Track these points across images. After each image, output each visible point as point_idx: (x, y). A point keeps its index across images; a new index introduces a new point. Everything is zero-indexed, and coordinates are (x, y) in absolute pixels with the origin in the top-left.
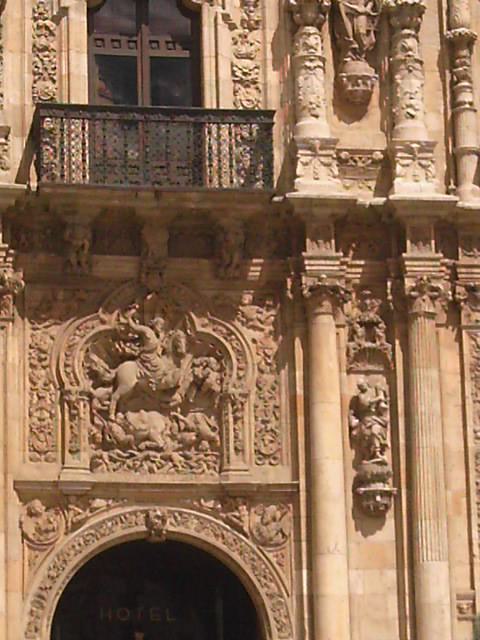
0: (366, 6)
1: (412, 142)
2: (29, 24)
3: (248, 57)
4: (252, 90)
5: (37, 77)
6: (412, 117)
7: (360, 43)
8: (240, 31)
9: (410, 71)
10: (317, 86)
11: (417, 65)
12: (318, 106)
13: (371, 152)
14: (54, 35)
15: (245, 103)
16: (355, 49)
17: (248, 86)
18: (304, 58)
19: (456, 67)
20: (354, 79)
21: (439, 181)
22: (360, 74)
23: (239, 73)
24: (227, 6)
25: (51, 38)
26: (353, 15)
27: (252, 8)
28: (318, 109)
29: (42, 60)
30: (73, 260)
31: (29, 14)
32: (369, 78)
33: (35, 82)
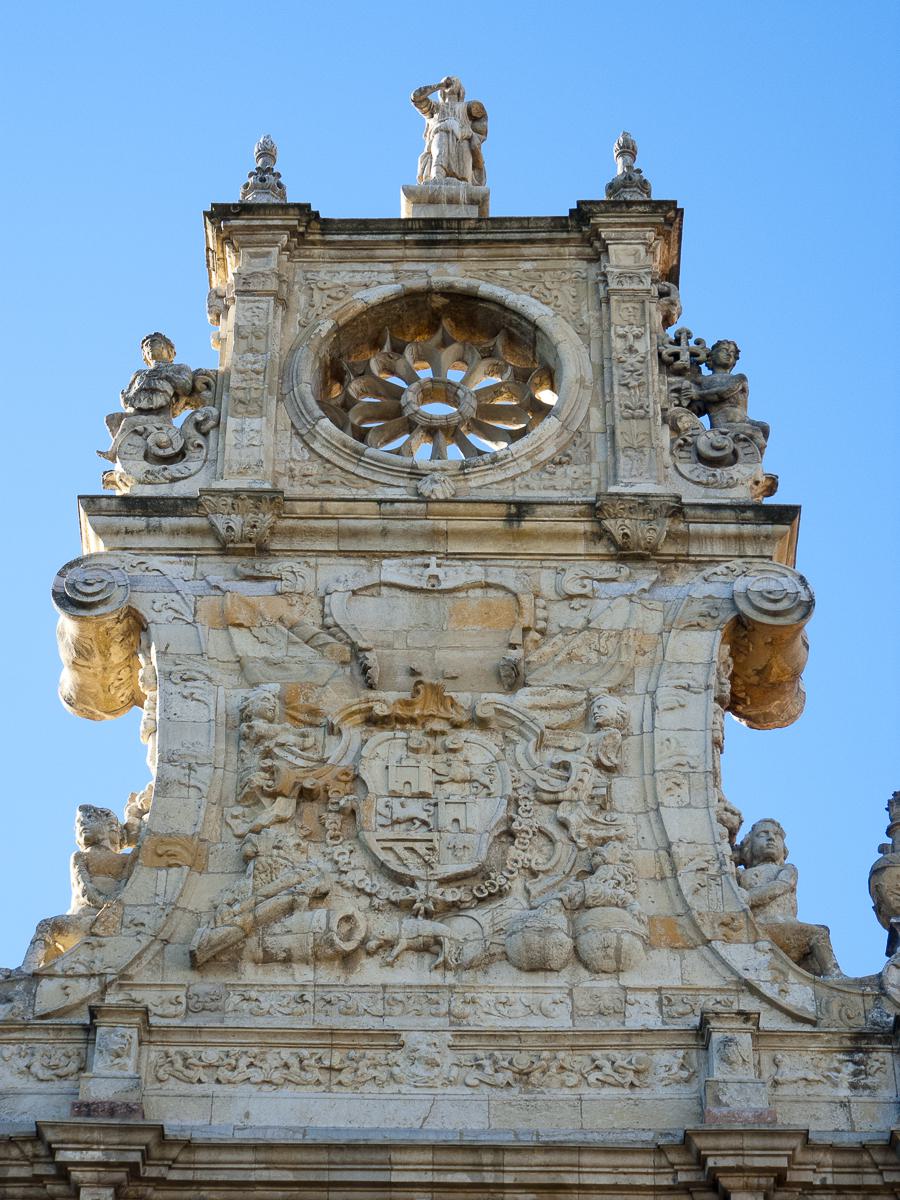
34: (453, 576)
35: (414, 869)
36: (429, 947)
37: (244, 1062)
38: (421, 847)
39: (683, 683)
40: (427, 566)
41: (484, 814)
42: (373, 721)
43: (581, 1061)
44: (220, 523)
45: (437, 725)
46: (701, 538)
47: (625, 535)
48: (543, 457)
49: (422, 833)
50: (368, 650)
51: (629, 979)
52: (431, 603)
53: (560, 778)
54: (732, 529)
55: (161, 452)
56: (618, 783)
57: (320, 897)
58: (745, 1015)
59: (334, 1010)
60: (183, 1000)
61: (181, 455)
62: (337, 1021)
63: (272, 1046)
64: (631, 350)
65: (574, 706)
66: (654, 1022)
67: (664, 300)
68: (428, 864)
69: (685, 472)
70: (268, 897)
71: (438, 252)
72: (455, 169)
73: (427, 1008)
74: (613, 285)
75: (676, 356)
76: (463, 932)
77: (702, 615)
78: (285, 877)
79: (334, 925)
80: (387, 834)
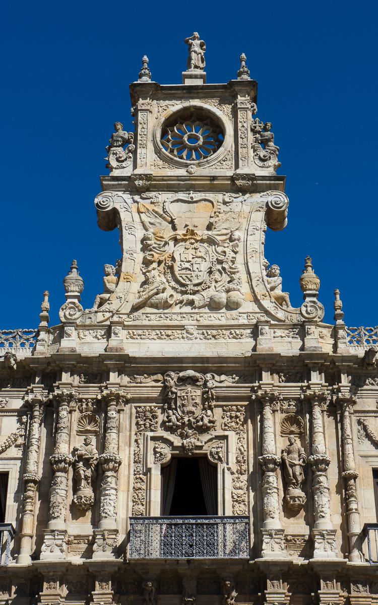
0: (299, 460)
1: (324, 530)
2: (132, 477)
3: (240, 488)
4: (242, 505)
5: (135, 503)
6: (323, 517)
7: (297, 481)
8: (237, 475)
9: (321, 493)
10: (274, 502)
11: (326, 490)
12: (273, 512)
13: (304, 536)
14: (144, 482)
15: (239, 512)
16: (294, 482)
17: (239, 503)
18: (267, 488)
19: (348, 491)
20: (293, 498)
21: (338, 550)
22: (296, 496)
23: (235, 497)
24: (230, 463)
25: (142, 483)
26: (293, 465)
27: (242, 464)
28: (274, 514)
29: (137, 495)
30: (147, 599)
31: (132, 472)
32: (301, 497)
33: (133, 506)
34: (197, 196)
35: (189, 283)
36: (191, 303)
37: (147, 333)
38: (189, 276)
39: (255, 227)
40: (189, 194)
41: (204, 266)
42: (176, 240)
43: (227, 332)
45: (193, 241)
47: (241, 185)
49: (189, 272)
50: (175, 219)
51: (240, 310)
53: (223, 255)
55: (120, 159)
56: (238, 256)
58: (267, 322)
59: (168, 319)
60: (132, 317)
62: (168, 322)
63: (154, 330)
64: (243, 126)
65: (228, 234)
66: (246, 322)
67: (252, 109)
68: (191, 281)
69: (257, 163)
70: (152, 290)
72: (197, 64)
73: (191, 319)
74: (239, 106)
75: (255, 127)
77: (260, 207)
78: (156, 285)
79: (168, 297)
80: (180, 272)
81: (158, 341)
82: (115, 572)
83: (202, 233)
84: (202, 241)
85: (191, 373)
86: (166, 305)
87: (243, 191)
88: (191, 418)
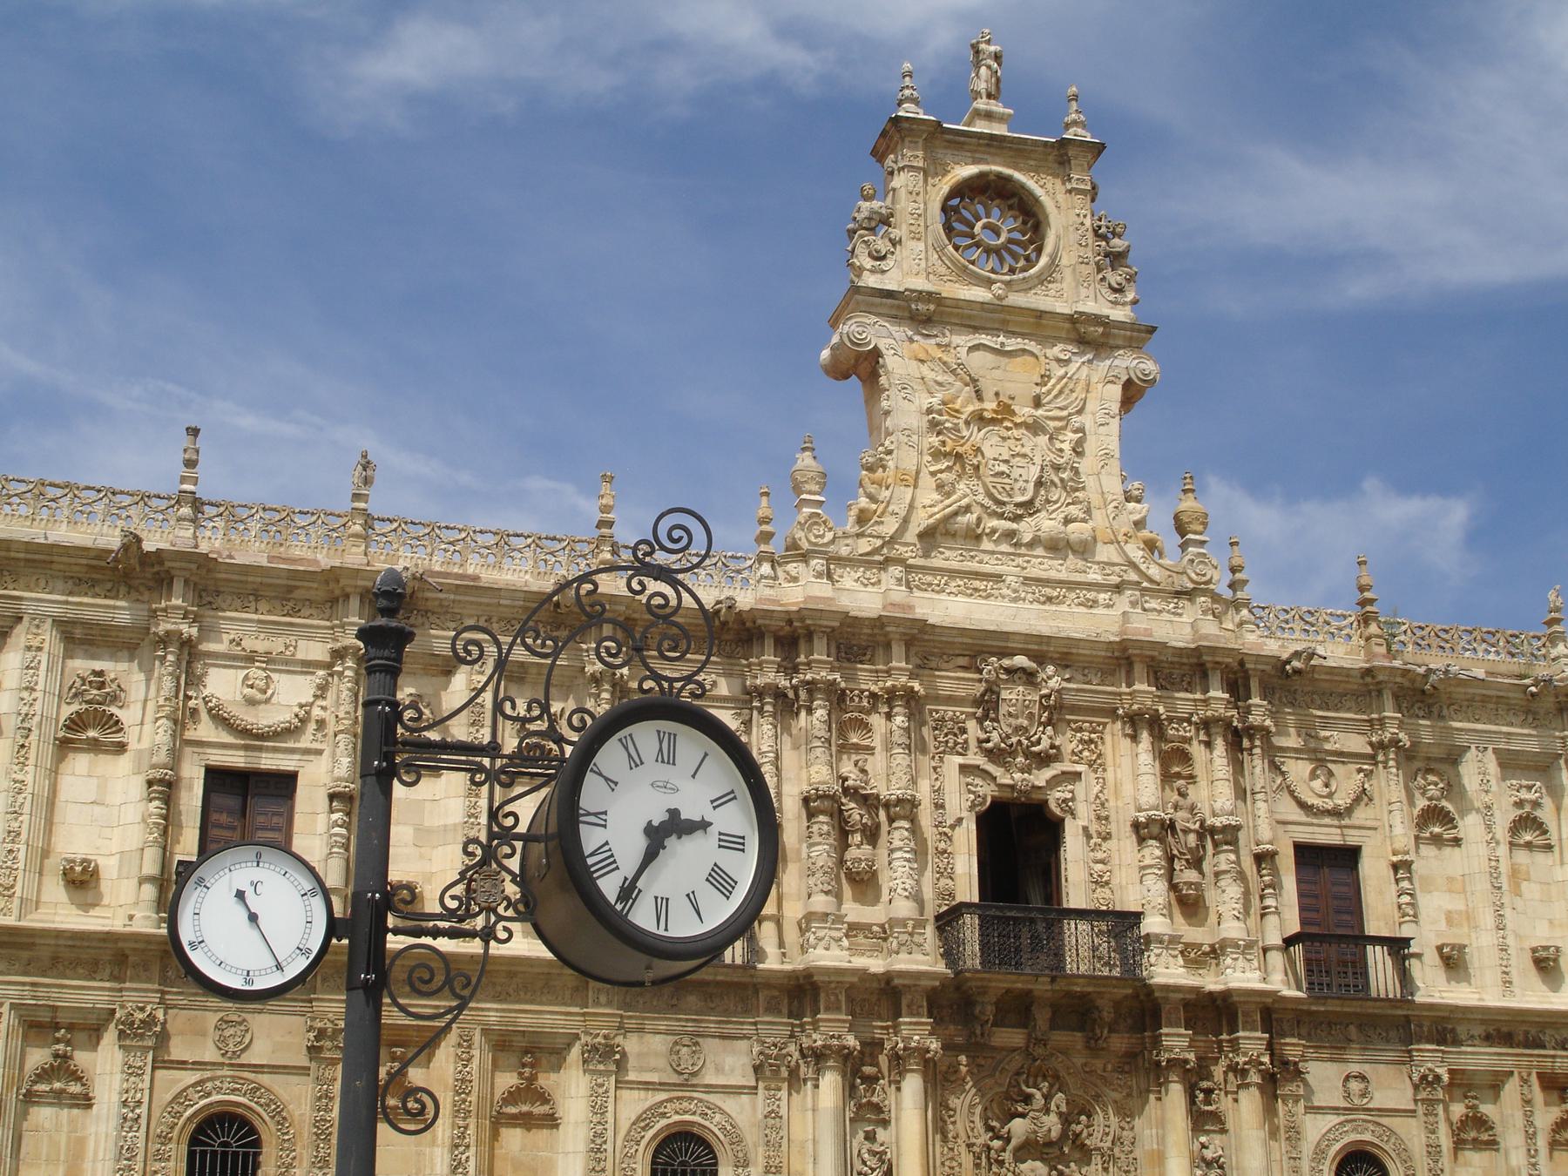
13: (1202, 945)
34: (1013, 344)
36: (1010, 535)
38: (1008, 487)
41: (1034, 472)
44: (913, 306)
45: (1010, 425)
46: (1115, 336)
48: (1043, 277)
52: (1004, 360)
54: (1128, 333)
57: (967, 509)
61: (883, 258)
62: (973, 566)
64: (1082, 224)
68: (1010, 496)
71: (992, 150)
75: (1100, 227)
76: (1026, 529)
81: (960, 598)
82: (934, 989)
83: (1024, 412)
84: (1025, 425)
85: (1021, 661)
86: (974, 536)
87: (1083, 342)
88: (1022, 739)
